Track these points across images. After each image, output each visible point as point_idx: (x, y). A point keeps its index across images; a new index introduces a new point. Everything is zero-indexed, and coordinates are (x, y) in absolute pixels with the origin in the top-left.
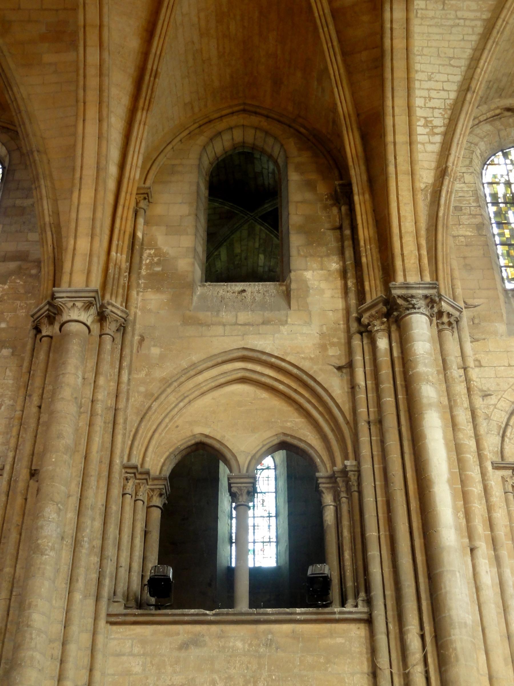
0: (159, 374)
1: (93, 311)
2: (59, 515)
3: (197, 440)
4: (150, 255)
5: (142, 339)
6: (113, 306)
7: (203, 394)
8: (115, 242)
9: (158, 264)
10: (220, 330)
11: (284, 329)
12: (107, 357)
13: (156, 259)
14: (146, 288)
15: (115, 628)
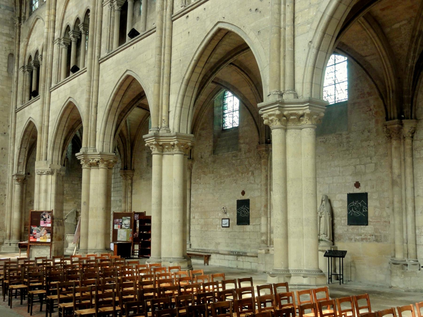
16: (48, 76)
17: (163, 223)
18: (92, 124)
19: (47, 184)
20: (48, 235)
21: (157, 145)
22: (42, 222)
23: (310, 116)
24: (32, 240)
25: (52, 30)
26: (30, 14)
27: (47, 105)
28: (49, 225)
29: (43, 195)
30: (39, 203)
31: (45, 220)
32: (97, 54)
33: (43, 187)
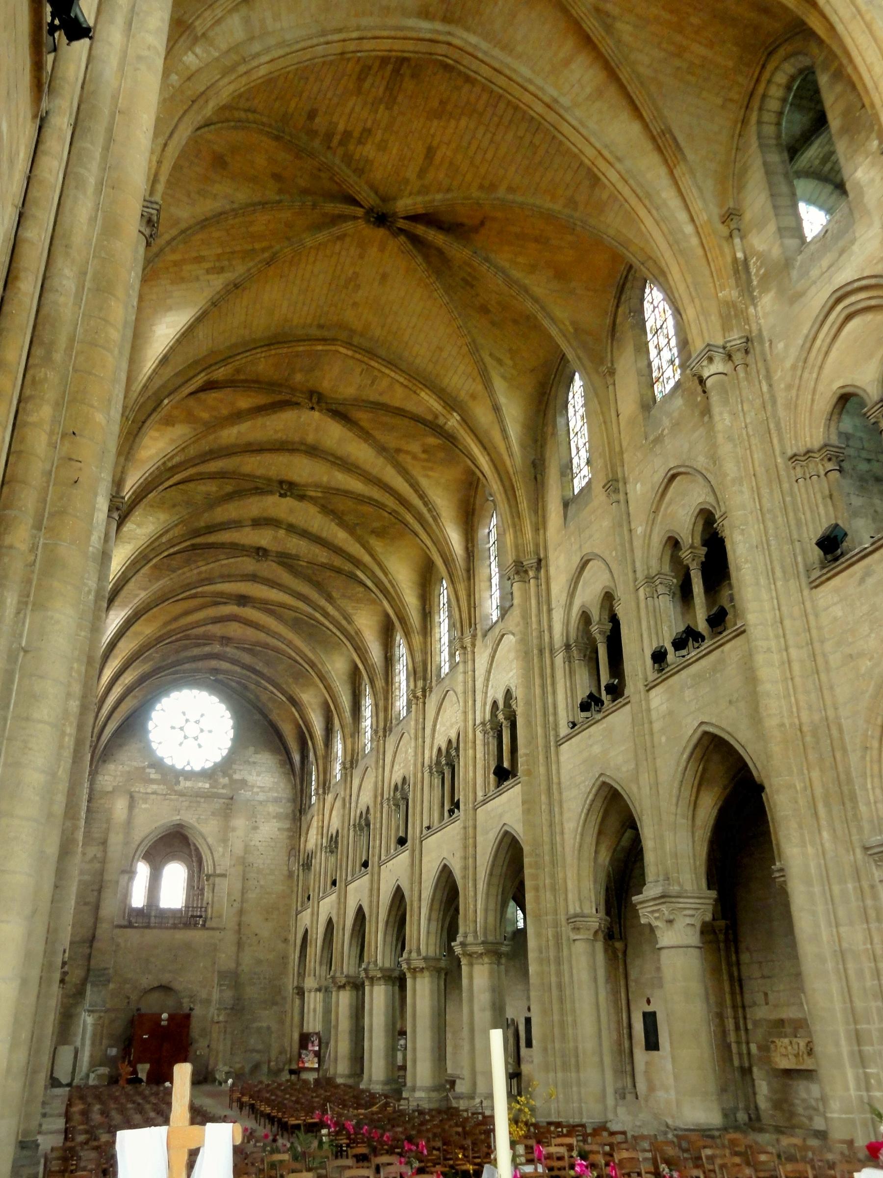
0: (788, 364)
1: (718, 358)
2: (743, 534)
3: (838, 395)
4: (755, 263)
5: (771, 341)
6: (730, 341)
7: (827, 353)
8: (717, 283)
9: (761, 267)
10: (813, 290)
11: (855, 248)
12: (744, 384)
13: (758, 264)
14: (760, 293)
15: (819, 589)
16: (317, 886)
17: (374, 1048)
18: (339, 946)
19: (315, 1001)
20: (316, 1060)
21: (367, 977)
22: (310, 1045)
23: (427, 969)
24: (301, 1065)
25: (320, 837)
26: (309, 807)
27: (315, 917)
28: (317, 1048)
29: (312, 1014)
30: (308, 1023)
31: (313, 1042)
32: (344, 877)
33: (312, 1006)
